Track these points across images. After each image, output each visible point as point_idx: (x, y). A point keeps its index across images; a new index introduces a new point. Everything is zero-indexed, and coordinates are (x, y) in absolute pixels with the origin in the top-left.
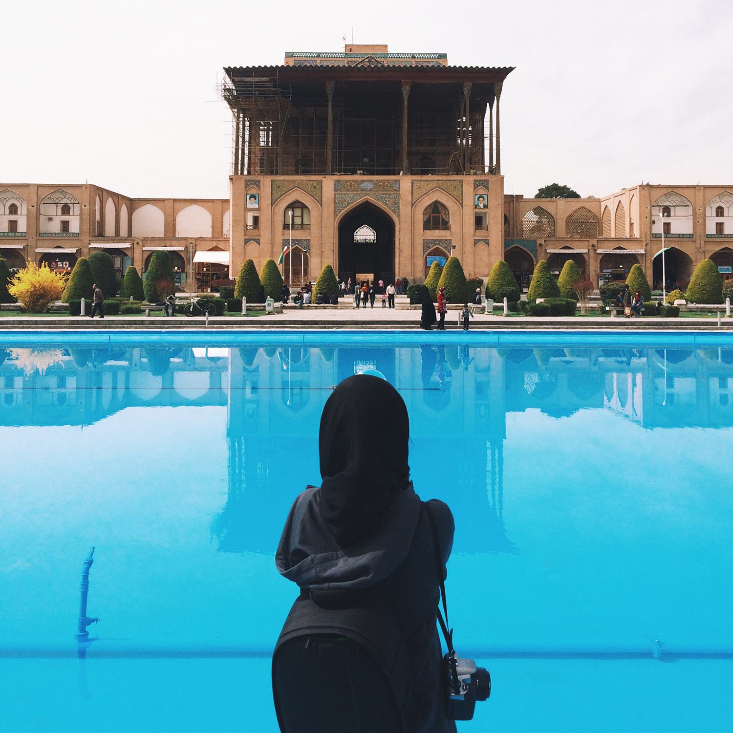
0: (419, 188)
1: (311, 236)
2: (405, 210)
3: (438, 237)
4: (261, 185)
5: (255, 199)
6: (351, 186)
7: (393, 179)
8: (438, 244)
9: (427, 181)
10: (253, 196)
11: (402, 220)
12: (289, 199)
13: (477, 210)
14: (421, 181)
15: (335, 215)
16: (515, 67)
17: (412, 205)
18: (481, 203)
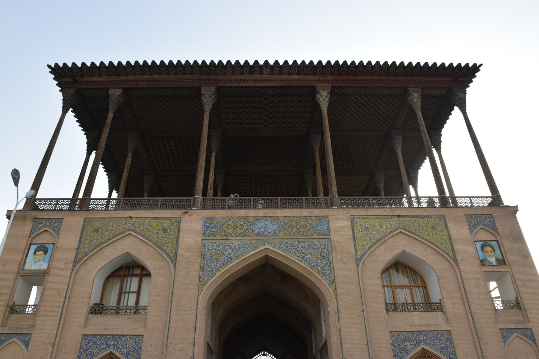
0: (367, 230)
1: (145, 326)
2: (344, 270)
3: (420, 325)
4: (63, 227)
5: (46, 252)
6: (236, 227)
7: (315, 214)
8: (425, 342)
9: (378, 217)
10: (42, 248)
11: (340, 289)
12: (112, 254)
13: (487, 269)
14: (367, 217)
15: (202, 281)
16: (481, 65)
17: (358, 261)
18: (489, 256)
